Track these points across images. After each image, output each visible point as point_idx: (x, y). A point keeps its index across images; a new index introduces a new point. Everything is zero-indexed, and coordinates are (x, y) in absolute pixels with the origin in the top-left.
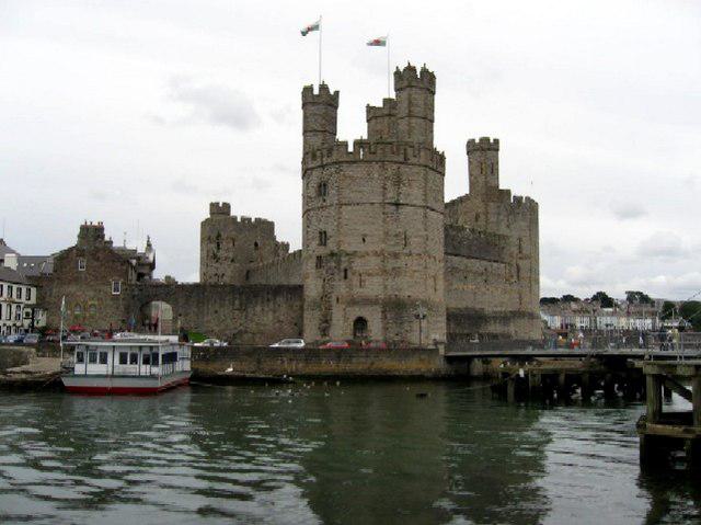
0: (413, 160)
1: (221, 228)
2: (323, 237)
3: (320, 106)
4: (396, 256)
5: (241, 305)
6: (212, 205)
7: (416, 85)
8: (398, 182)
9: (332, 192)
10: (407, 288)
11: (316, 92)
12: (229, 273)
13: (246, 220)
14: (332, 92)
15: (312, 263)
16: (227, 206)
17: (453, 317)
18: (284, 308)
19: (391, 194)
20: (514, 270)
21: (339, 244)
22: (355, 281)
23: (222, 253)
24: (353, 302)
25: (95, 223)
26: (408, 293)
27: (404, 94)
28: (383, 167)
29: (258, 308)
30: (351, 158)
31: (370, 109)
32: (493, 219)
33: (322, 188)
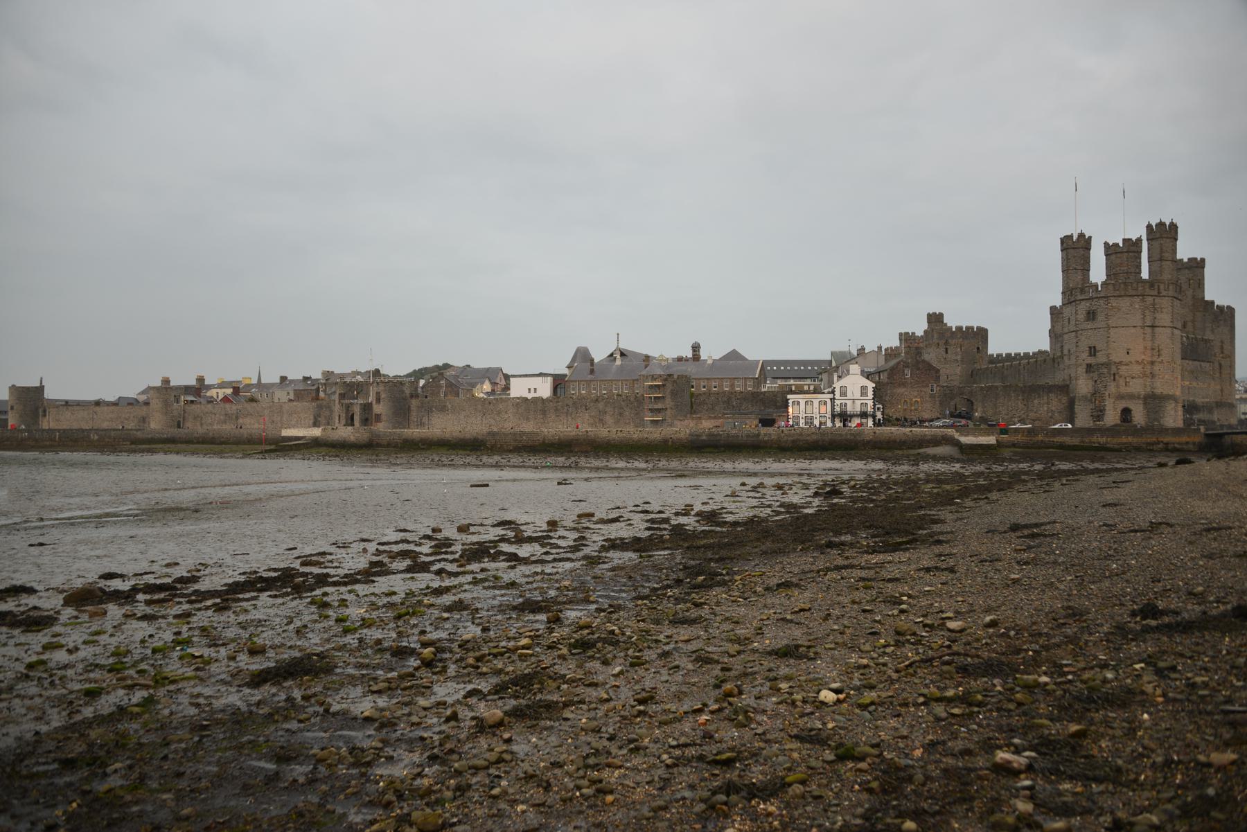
0: (1164, 293)
2: (1093, 351)
3: (1075, 250)
8: (1154, 308)
9: (1100, 317)
10: (1160, 389)
13: (959, 328)
15: (1082, 370)
17: (1190, 408)
18: (1055, 403)
19: (1148, 323)
20: (1217, 365)
21: (1108, 356)
22: (1122, 382)
23: (950, 356)
24: (1120, 397)
28: (1143, 300)
29: (1036, 401)
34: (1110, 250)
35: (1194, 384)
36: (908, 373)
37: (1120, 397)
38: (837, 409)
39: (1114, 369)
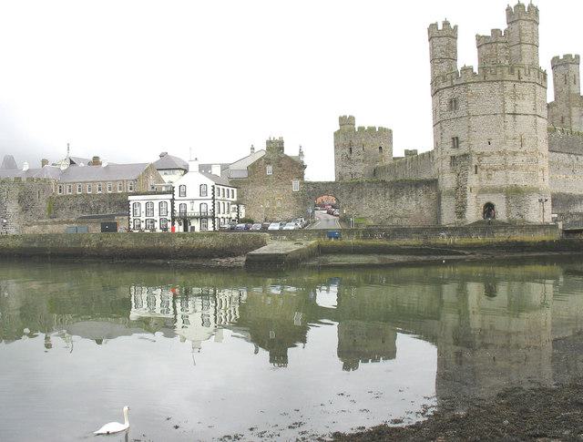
0: (525, 79)
1: (350, 138)
2: (456, 142)
3: (442, 38)
4: (515, 154)
5: (391, 196)
6: (341, 119)
7: (523, 17)
8: (515, 96)
9: (462, 106)
10: (520, 179)
11: (440, 27)
12: (360, 170)
14: (452, 27)
15: (446, 164)
16: (352, 118)
19: (509, 109)
22: (484, 174)
23: (353, 157)
24: (483, 191)
25: (277, 138)
26: (526, 183)
27: (515, 26)
29: (404, 198)
30: (476, 79)
31: (479, 38)
32: (575, 119)
33: (453, 104)
34: (482, 42)
35: (571, 177)
36: (269, 169)
37: (483, 191)
38: (177, 208)
39: (475, 161)
